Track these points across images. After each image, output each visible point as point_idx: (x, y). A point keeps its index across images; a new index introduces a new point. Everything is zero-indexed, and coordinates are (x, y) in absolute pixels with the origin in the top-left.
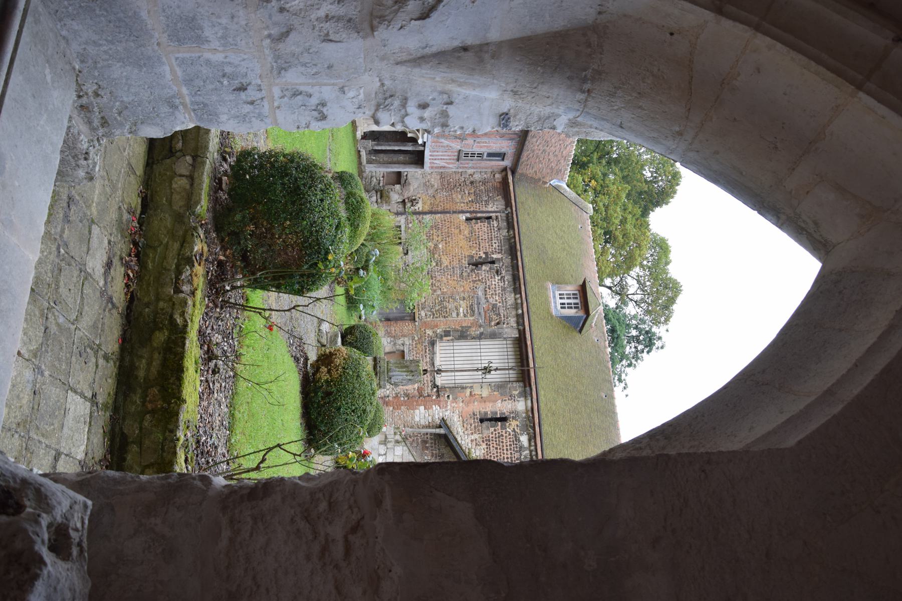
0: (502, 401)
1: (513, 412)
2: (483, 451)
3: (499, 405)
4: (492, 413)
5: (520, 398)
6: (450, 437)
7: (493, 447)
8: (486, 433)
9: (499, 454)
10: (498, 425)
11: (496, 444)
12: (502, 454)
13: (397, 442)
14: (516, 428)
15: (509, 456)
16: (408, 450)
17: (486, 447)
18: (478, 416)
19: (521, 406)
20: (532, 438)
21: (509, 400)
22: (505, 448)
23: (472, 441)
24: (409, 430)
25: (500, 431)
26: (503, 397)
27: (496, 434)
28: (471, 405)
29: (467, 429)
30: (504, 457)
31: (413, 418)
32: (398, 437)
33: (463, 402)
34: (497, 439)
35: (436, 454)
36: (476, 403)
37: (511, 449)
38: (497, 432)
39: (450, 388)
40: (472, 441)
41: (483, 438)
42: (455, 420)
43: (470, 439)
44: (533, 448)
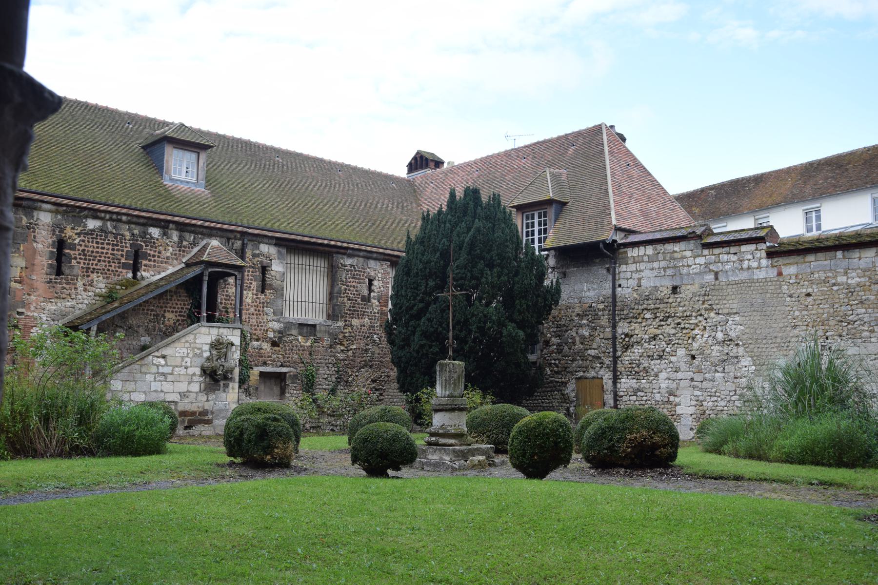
2: (101, 278)
3: (40, 246)
4: (50, 258)
5: (33, 217)
7: (96, 265)
8: (77, 271)
9: (107, 259)
10: (69, 254)
11: (93, 260)
12: (107, 256)
14: (76, 231)
15: (111, 247)
17: (95, 274)
18: (53, 277)
19: (45, 218)
20: (95, 214)
21: (34, 232)
22: (100, 250)
23: (85, 290)
25: (77, 253)
27: (80, 259)
29: (70, 295)
30: (111, 254)
33: (29, 295)
34: (88, 257)
36: (34, 277)
37: (102, 244)
38: (78, 257)
40: (85, 290)
41: (84, 276)
42: (54, 308)
44: (108, 216)
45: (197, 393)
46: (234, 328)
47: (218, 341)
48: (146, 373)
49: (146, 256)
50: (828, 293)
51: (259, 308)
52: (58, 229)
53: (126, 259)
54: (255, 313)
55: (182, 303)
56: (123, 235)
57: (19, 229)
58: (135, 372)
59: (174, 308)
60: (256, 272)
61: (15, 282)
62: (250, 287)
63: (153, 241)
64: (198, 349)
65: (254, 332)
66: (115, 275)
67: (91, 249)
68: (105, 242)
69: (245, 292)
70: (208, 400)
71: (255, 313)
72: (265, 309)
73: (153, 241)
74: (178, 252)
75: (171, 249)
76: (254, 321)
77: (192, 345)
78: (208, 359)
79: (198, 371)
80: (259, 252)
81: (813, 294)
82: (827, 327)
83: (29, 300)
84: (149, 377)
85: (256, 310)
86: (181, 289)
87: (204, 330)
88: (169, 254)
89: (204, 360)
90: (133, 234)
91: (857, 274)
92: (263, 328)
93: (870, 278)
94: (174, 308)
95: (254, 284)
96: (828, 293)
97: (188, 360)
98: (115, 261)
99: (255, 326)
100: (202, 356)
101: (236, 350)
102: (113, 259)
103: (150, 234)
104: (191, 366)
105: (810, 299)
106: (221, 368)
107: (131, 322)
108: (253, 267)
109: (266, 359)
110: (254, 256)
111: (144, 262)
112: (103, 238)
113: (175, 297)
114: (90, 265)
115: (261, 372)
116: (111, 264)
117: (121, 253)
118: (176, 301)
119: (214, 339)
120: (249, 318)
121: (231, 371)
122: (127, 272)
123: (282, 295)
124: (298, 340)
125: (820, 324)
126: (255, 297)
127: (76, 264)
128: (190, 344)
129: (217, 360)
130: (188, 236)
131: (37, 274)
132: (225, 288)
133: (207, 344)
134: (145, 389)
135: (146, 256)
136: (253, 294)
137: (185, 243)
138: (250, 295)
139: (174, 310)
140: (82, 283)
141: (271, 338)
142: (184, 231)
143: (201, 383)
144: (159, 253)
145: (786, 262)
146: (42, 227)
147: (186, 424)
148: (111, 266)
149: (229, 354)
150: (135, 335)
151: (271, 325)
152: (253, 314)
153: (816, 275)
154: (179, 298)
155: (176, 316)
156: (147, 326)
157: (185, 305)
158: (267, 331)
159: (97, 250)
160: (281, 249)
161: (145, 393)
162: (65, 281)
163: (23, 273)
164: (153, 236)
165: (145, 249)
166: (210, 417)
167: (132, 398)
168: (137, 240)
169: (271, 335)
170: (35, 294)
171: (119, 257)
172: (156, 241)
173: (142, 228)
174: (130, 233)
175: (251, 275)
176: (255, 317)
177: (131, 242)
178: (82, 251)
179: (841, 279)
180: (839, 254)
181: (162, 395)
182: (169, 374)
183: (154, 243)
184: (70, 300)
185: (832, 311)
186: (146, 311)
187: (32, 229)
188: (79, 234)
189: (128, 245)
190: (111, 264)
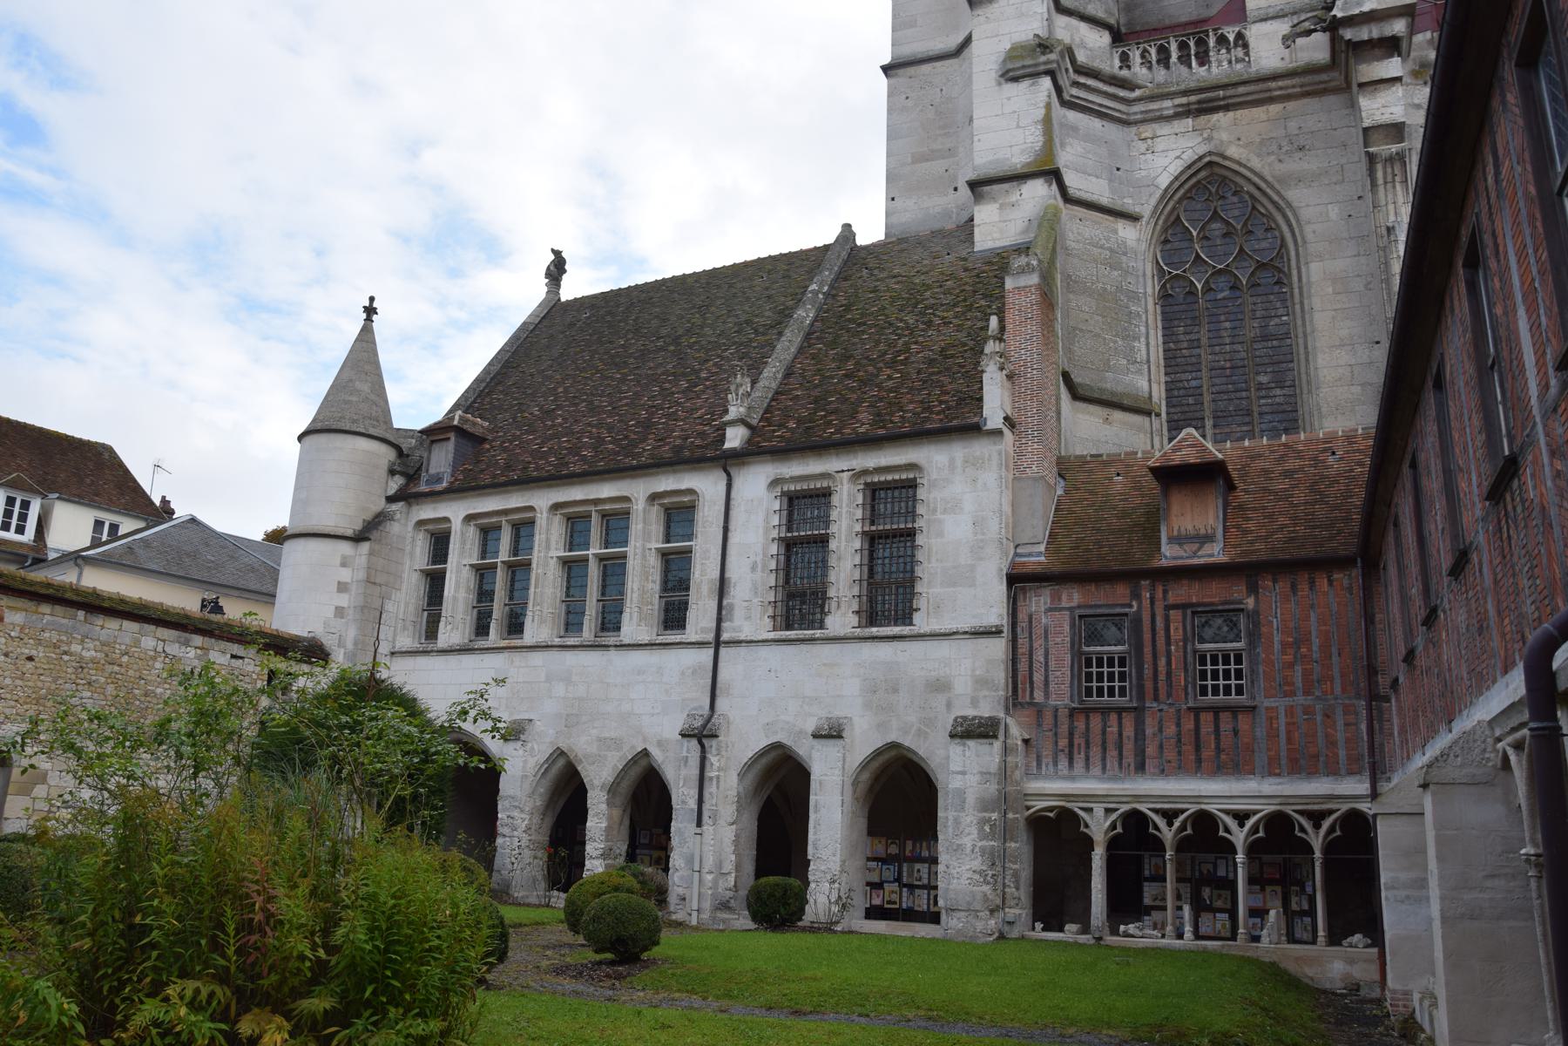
50: (55, 662)
81: (37, 659)
82: (41, 708)
91: (95, 646)
93: (107, 656)
96: (55, 662)
105: (30, 665)
125: (34, 702)
145: (10, 605)
153: (47, 635)
179: (76, 648)
180: (81, 614)
185: (53, 687)
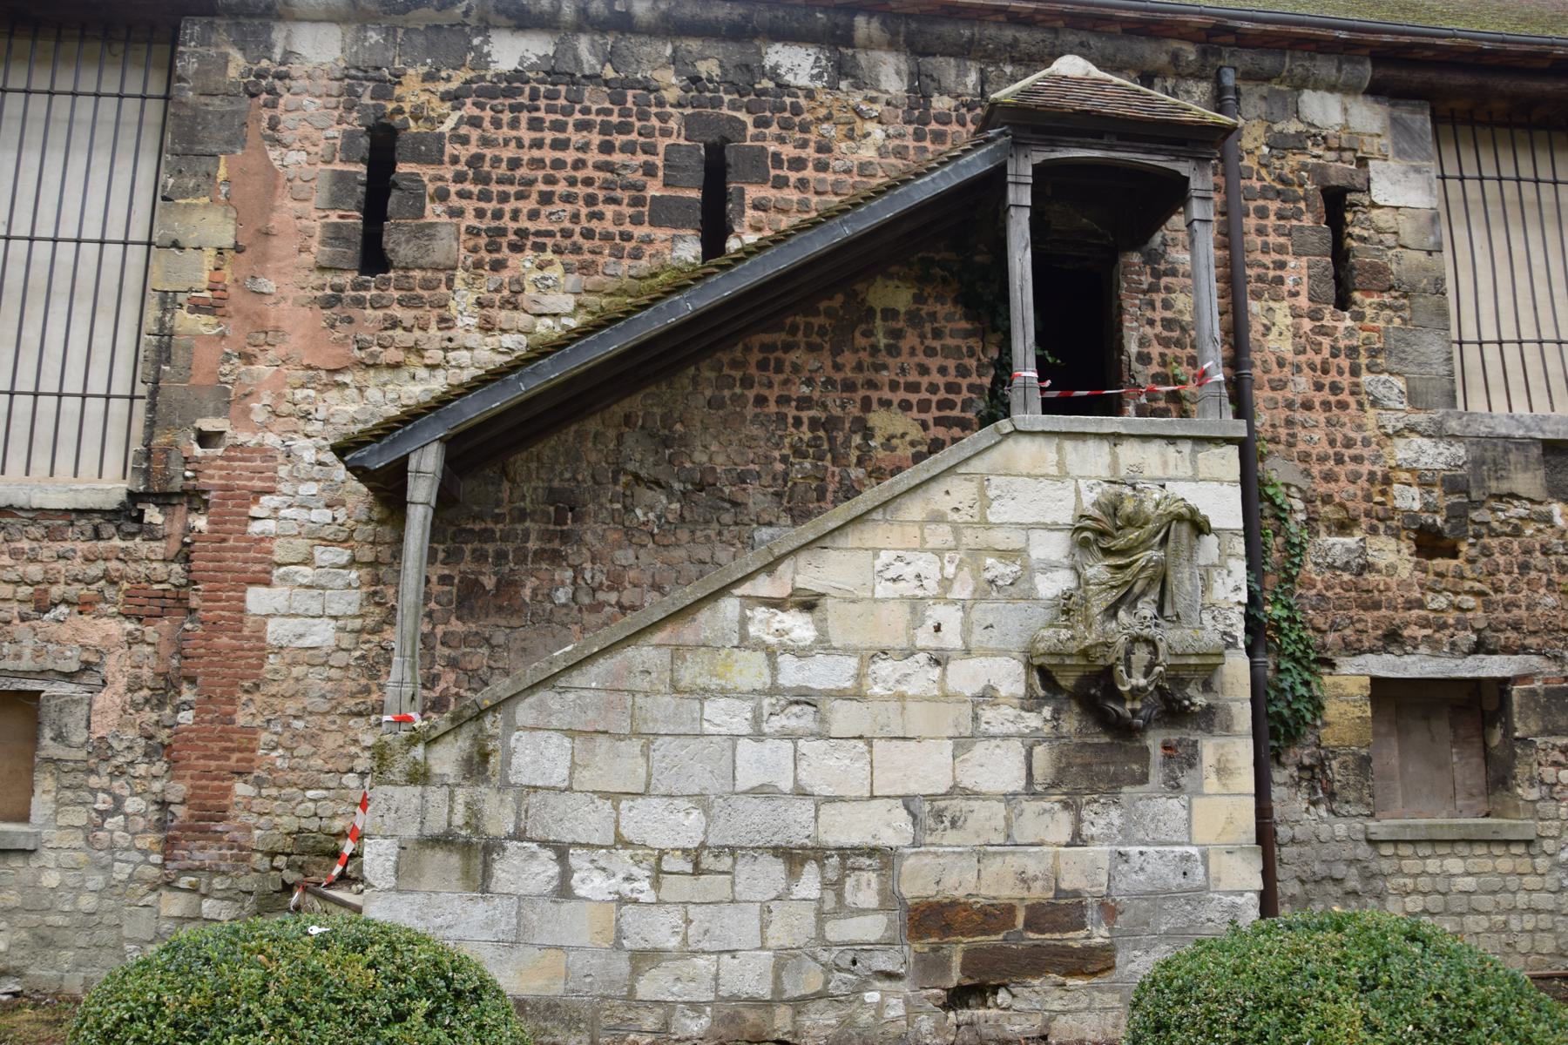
0: (278, 142)
1: (351, 91)
2: (556, 272)
3: (293, 157)
4: (335, 202)
5: (269, 47)
6: (473, 410)
7: (534, 215)
8: (449, 245)
9: (581, 190)
10: (415, 178)
11: (520, 196)
12: (580, 175)
13: (477, 765)
14: (442, 87)
15: (596, 138)
16: (547, 696)
18: (348, 278)
21: (274, 106)
22: (548, 155)
23: (487, 327)
24: (400, 678)
25: (448, 172)
26: (252, 134)
27: (462, 195)
28: (273, 312)
29: (417, 350)
30: (598, 167)
31: (316, 658)
32: (446, 759)
33: (248, 358)
34: (495, 188)
35: (547, 536)
36: (267, 285)
37: (559, 126)
38: (453, 188)
39: (151, 425)
40: (487, 327)
41: (478, 265)
42: (352, 408)
43: (476, 337)
45: (1009, 798)
46: (1200, 441)
47: (1112, 508)
48: (704, 694)
49: (759, 166)
51: (1333, 376)
52: (371, 85)
53: (666, 185)
54: (1318, 398)
55: (951, 364)
56: (647, 87)
57: (217, 101)
58: (646, 686)
59: (913, 387)
60: (1298, 215)
61: (191, 311)
62: (1280, 281)
63: (788, 100)
64: (1005, 554)
65: (1323, 488)
66: (618, 254)
67: (508, 153)
68: (571, 121)
69: (1254, 306)
70: (1077, 839)
71: (1318, 398)
72: (1365, 378)
73: (788, 100)
74: (910, 143)
75: (878, 133)
76: (1315, 438)
77: (969, 538)
78: (1067, 608)
79: (1010, 677)
80: (1301, 127)
83: (247, 380)
84: (724, 716)
85: (1319, 387)
86: (940, 299)
87: (1025, 452)
88: (868, 153)
89: (1041, 615)
90: (695, 80)
92: (1365, 468)
94: (913, 387)
95: (1297, 270)
97: (951, 618)
98: (618, 193)
99: (1322, 459)
100: (1030, 597)
101: (1224, 554)
102: (607, 186)
103: (774, 74)
104: (968, 652)
106: (1141, 655)
107: (701, 457)
108: (1279, 193)
109: (1399, 616)
110: (1281, 145)
111: (753, 192)
112: (562, 102)
113: (911, 339)
114: (506, 222)
115: (1376, 681)
116: (600, 207)
117: (641, 158)
118: (921, 358)
119: (1088, 498)
120: (1289, 423)
121: (1207, 672)
122: (673, 239)
123: (1444, 314)
124: (1548, 519)
126: (1307, 324)
127: (445, 219)
128: (956, 530)
129: (1112, 612)
130: (953, 73)
131: (278, 271)
132: (1153, 288)
133: (1053, 527)
134: (702, 779)
135: (759, 166)
136: (1296, 314)
137: (941, 103)
138: (1282, 317)
139: (914, 398)
140: (472, 298)
141: (1411, 516)
142: (926, 53)
143: (1030, 743)
144: (824, 148)
146: (304, 83)
147: (955, 978)
148: (600, 216)
149: (1184, 580)
150: (727, 518)
151: (1403, 451)
152: (1308, 406)
154: (937, 344)
155: (924, 425)
156: (786, 474)
157: (963, 371)
158: (1387, 481)
159: (536, 153)
160: (1404, 113)
161: (701, 801)
162: (397, 294)
163: (227, 270)
164: (789, 78)
165: (755, 138)
166: (1099, 935)
167: (628, 832)
168: (717, 103)
169: (1408, 498)
170: (272, 353)
171: (638, 176)
172: (803, 102)
173: (734, 52)
174: (678, 73)
175: (1278, 230)
176: (1319, 416)
177: (689, 111)
178: (469, 164)
181: (804, 810)
182: (842, 695)
183: (796, 110)
184: (422, 373)
186: (772, 408)
187: (264, 96)
188: (455, 98)
189: (673, 124)
190: (600, 207)
